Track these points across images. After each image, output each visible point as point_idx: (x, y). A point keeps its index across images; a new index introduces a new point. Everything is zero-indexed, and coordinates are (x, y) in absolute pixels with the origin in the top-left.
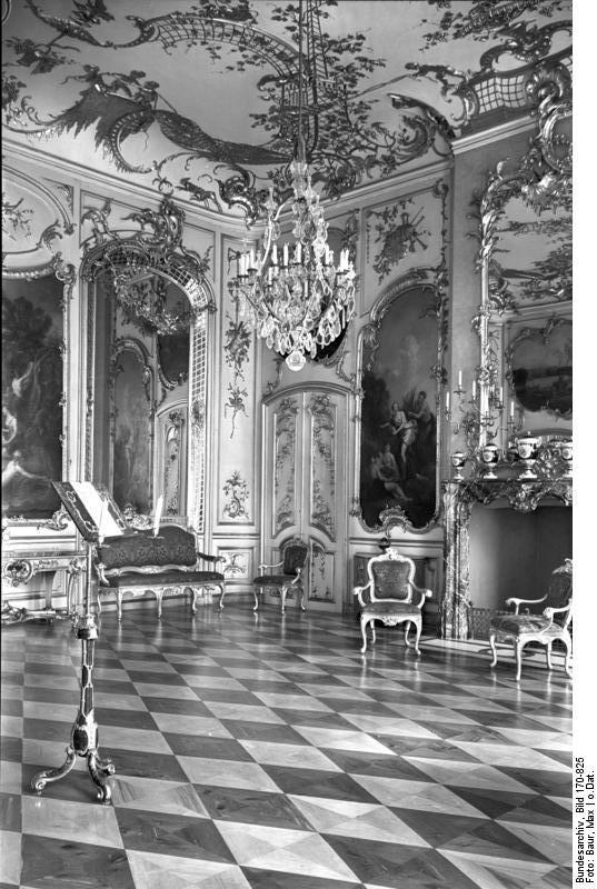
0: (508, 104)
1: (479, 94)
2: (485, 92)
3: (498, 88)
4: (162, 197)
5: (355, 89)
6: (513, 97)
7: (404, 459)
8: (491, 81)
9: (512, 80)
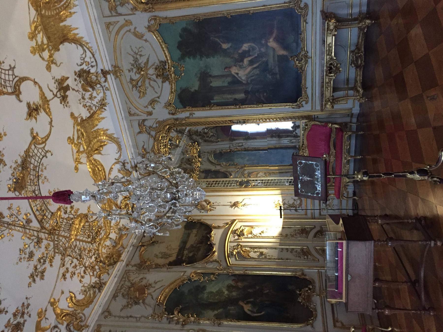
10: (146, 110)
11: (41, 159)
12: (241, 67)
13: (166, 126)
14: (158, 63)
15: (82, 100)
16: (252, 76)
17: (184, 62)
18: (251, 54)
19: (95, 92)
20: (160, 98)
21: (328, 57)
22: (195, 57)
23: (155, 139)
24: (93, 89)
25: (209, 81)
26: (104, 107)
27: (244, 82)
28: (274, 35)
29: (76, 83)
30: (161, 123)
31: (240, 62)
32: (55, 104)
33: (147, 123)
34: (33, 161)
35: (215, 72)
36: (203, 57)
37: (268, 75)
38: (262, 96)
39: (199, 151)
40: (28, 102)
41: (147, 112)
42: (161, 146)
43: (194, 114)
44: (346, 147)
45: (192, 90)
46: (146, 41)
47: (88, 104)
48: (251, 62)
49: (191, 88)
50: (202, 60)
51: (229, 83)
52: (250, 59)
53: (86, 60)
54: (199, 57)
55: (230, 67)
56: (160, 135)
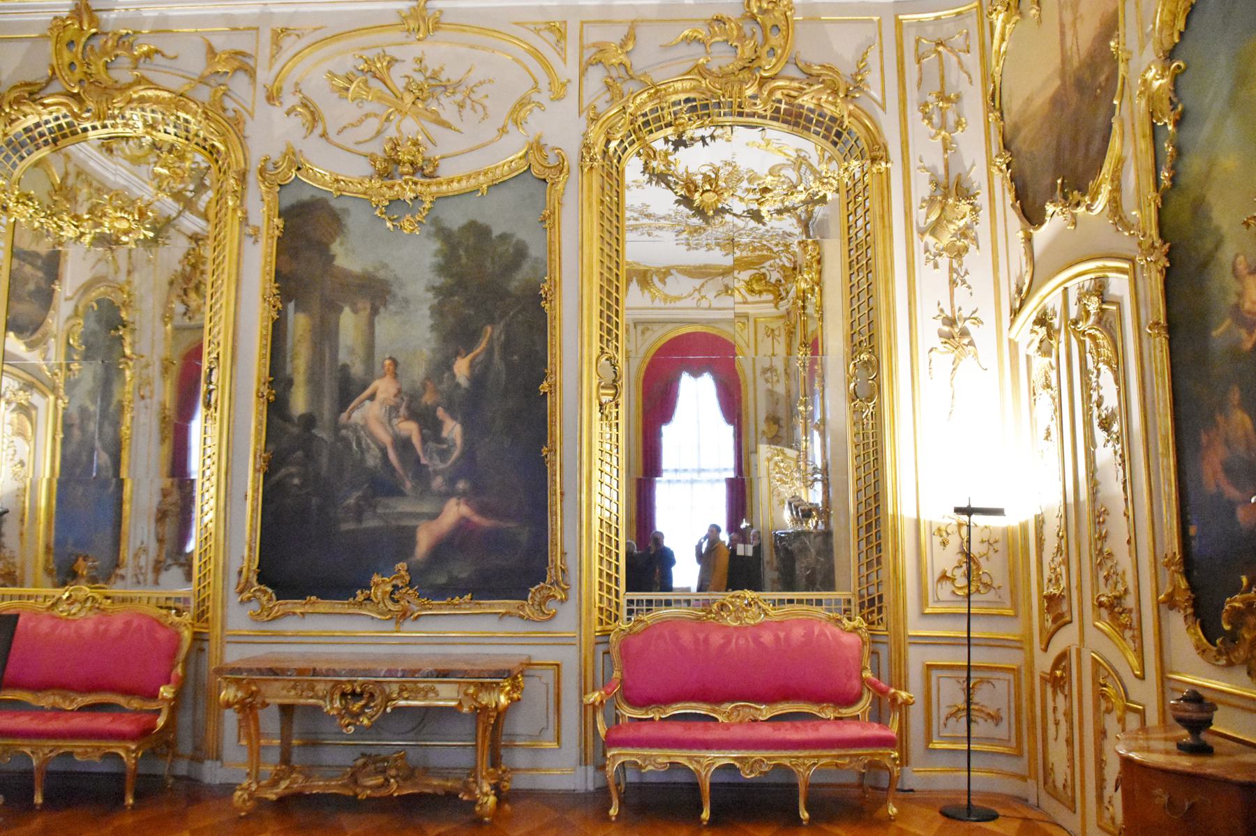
10: (288, 87)
12: (393, 410)
13: (225, 143)
14: (435, 153)
16: (359, 444)
17: (429, 235)
18: (431, 444)
20: (323, 141)
21: (395, 688)
22: (442, 269)
23: (181, 99)
25: (360, 305)
27: (344, 416)
28: (476, 519)
30: (235, 126)
31: (408, 408)
33: (240, 84)
35: (386, 328)
36: (436, 296)
37: (360, 493)
38: (293, 470)
39: (118, 242)
41: (280, 90)
42: (153, 111)
43: (256, 241)
44: (79, 750)
45: (336, 248)
46: (503, 131)
48: (403, 445)
49: (342, 244)
50: (428, 290)
51: (345, 368)
52: (416, 440)
54: (437, 284)
55: (395, 376)
56: (195, 114)
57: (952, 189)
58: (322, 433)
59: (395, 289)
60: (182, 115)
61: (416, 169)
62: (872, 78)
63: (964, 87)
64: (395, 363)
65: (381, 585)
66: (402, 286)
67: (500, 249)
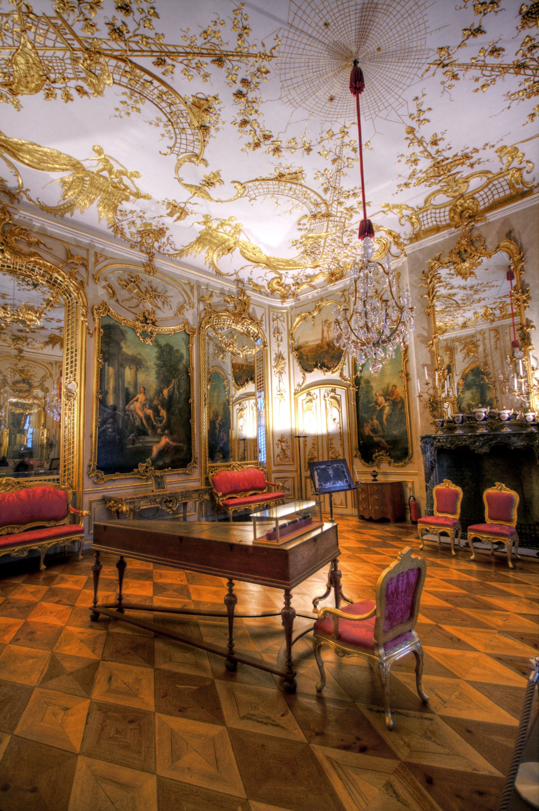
0: (439, 223)
1: (422, 219)
2: (425, 218)
3: (433, 215)
4: (239, 289)
5: (350, 222)
6: (442, 219)
7: (386, 423)
8: (429, 212)
9: (442, 210)
11: (176, 142)
12: (144, 405)
15: (141, 214)
16: (133, 417)
17: (154, 346)
18: (157, 418)
19: (135, 232)
22: (159, 358)
24: (139, 232)
26: (113, 228)
27: (127, 407)
28: (171, 443)
29: (161, 223)
31: (149, 405)
32: (181, 196)
33: (82, 270)
34: (190, 138)
35: (141, 377)
38: (109, 426)
40: (222, 185)
45: (122, 344)
47: (130, 216)
48: (148, 418)
51: (127, 389)
52: (152, 416)
53: (169, 245)
55: (145, 393)
57: (280, 357)
58: (120, 413)
59: (144, 363)
60: (56, 275)
61: (153, 323)
62: (264, 323)
63: (283, 331)
64: (144, 389)
65: (142, 467)
66: (146, 362)
67: (176, 354)
